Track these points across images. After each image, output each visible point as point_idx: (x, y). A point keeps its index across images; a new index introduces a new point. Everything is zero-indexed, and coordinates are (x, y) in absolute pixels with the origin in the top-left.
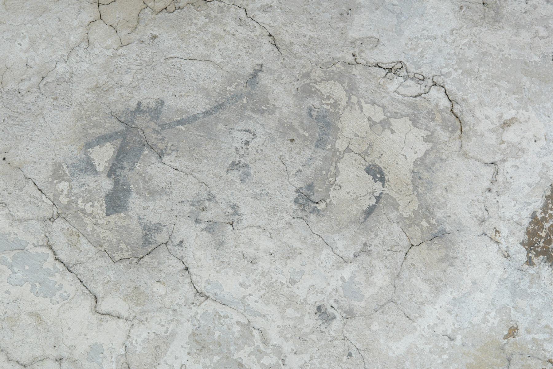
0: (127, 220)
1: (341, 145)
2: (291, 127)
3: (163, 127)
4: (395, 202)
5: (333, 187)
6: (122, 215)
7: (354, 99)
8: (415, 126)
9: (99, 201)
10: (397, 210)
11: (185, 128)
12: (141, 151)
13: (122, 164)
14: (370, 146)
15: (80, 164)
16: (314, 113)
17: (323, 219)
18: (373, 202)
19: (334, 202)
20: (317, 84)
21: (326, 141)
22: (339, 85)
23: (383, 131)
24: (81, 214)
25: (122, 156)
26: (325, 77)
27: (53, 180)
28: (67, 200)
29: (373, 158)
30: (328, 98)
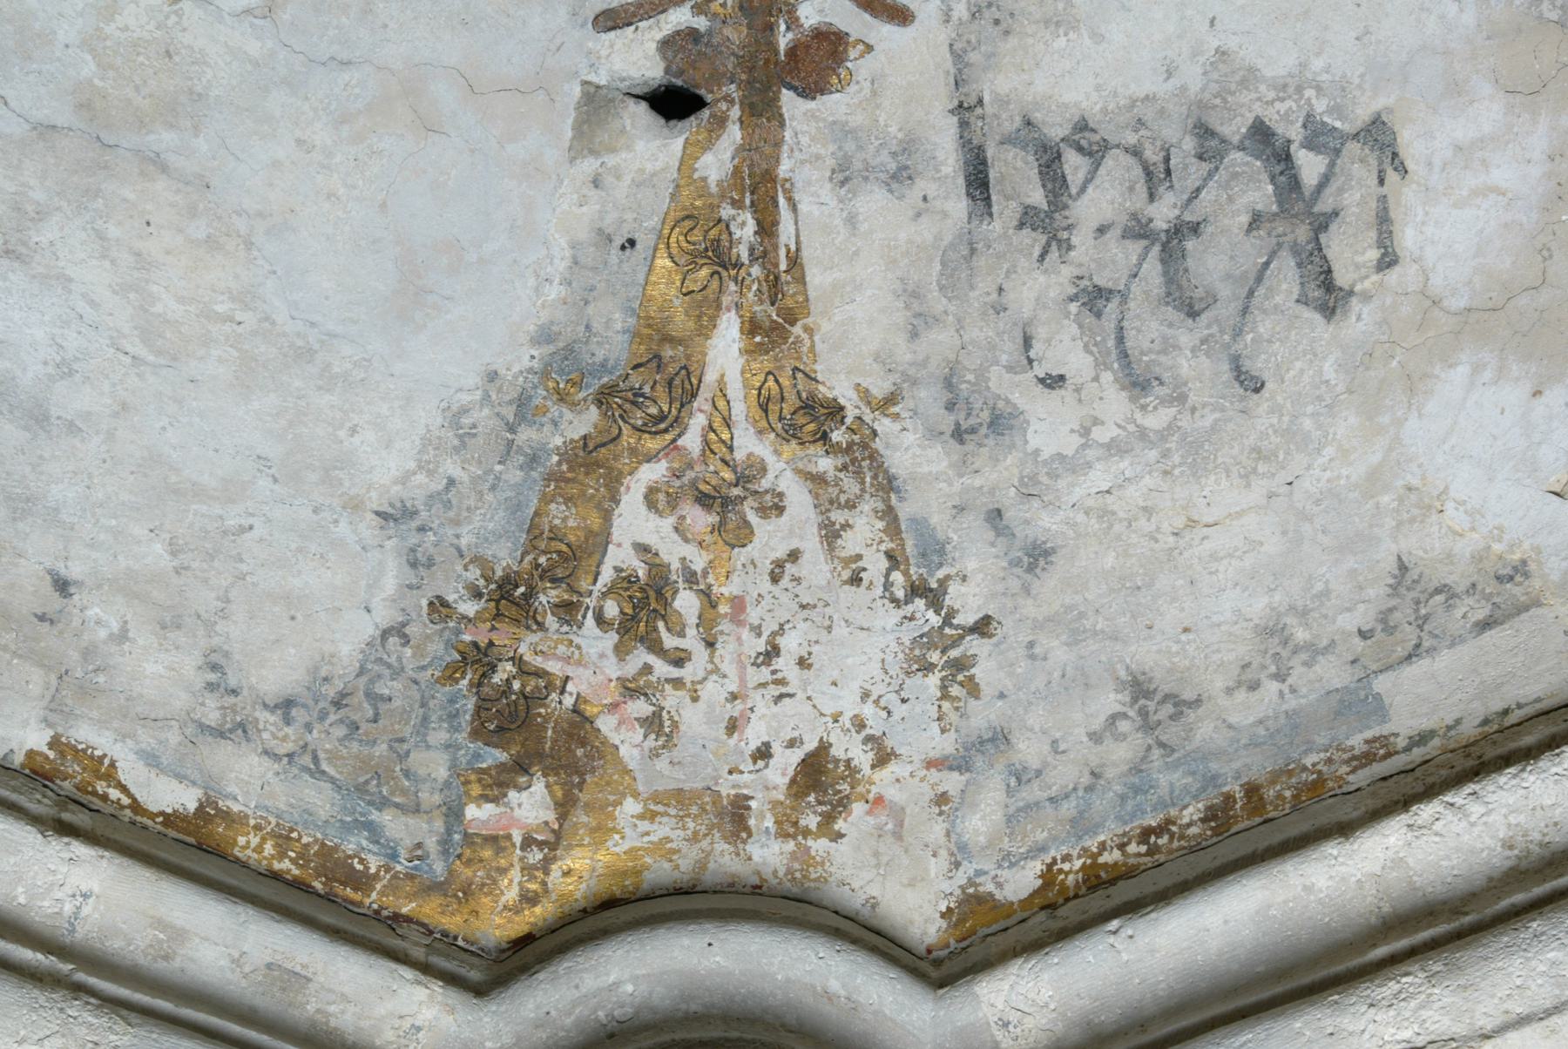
1: (1107, 377)
2: (1164, 352)
3: (1279, 245)
6: (1244, 130)
7: (1131, 428)
8: (1058, 454)
10: (1004, 367)
12: (1280, 204)
14: (1080, 400)
16: (1155, 383)
17: (1062, 297)
18: (1032, 354)
19: (1066, 322)
24: (1281, 95)
28: (1306, 96)
29: (1066, 393)
30: (1155, 408)
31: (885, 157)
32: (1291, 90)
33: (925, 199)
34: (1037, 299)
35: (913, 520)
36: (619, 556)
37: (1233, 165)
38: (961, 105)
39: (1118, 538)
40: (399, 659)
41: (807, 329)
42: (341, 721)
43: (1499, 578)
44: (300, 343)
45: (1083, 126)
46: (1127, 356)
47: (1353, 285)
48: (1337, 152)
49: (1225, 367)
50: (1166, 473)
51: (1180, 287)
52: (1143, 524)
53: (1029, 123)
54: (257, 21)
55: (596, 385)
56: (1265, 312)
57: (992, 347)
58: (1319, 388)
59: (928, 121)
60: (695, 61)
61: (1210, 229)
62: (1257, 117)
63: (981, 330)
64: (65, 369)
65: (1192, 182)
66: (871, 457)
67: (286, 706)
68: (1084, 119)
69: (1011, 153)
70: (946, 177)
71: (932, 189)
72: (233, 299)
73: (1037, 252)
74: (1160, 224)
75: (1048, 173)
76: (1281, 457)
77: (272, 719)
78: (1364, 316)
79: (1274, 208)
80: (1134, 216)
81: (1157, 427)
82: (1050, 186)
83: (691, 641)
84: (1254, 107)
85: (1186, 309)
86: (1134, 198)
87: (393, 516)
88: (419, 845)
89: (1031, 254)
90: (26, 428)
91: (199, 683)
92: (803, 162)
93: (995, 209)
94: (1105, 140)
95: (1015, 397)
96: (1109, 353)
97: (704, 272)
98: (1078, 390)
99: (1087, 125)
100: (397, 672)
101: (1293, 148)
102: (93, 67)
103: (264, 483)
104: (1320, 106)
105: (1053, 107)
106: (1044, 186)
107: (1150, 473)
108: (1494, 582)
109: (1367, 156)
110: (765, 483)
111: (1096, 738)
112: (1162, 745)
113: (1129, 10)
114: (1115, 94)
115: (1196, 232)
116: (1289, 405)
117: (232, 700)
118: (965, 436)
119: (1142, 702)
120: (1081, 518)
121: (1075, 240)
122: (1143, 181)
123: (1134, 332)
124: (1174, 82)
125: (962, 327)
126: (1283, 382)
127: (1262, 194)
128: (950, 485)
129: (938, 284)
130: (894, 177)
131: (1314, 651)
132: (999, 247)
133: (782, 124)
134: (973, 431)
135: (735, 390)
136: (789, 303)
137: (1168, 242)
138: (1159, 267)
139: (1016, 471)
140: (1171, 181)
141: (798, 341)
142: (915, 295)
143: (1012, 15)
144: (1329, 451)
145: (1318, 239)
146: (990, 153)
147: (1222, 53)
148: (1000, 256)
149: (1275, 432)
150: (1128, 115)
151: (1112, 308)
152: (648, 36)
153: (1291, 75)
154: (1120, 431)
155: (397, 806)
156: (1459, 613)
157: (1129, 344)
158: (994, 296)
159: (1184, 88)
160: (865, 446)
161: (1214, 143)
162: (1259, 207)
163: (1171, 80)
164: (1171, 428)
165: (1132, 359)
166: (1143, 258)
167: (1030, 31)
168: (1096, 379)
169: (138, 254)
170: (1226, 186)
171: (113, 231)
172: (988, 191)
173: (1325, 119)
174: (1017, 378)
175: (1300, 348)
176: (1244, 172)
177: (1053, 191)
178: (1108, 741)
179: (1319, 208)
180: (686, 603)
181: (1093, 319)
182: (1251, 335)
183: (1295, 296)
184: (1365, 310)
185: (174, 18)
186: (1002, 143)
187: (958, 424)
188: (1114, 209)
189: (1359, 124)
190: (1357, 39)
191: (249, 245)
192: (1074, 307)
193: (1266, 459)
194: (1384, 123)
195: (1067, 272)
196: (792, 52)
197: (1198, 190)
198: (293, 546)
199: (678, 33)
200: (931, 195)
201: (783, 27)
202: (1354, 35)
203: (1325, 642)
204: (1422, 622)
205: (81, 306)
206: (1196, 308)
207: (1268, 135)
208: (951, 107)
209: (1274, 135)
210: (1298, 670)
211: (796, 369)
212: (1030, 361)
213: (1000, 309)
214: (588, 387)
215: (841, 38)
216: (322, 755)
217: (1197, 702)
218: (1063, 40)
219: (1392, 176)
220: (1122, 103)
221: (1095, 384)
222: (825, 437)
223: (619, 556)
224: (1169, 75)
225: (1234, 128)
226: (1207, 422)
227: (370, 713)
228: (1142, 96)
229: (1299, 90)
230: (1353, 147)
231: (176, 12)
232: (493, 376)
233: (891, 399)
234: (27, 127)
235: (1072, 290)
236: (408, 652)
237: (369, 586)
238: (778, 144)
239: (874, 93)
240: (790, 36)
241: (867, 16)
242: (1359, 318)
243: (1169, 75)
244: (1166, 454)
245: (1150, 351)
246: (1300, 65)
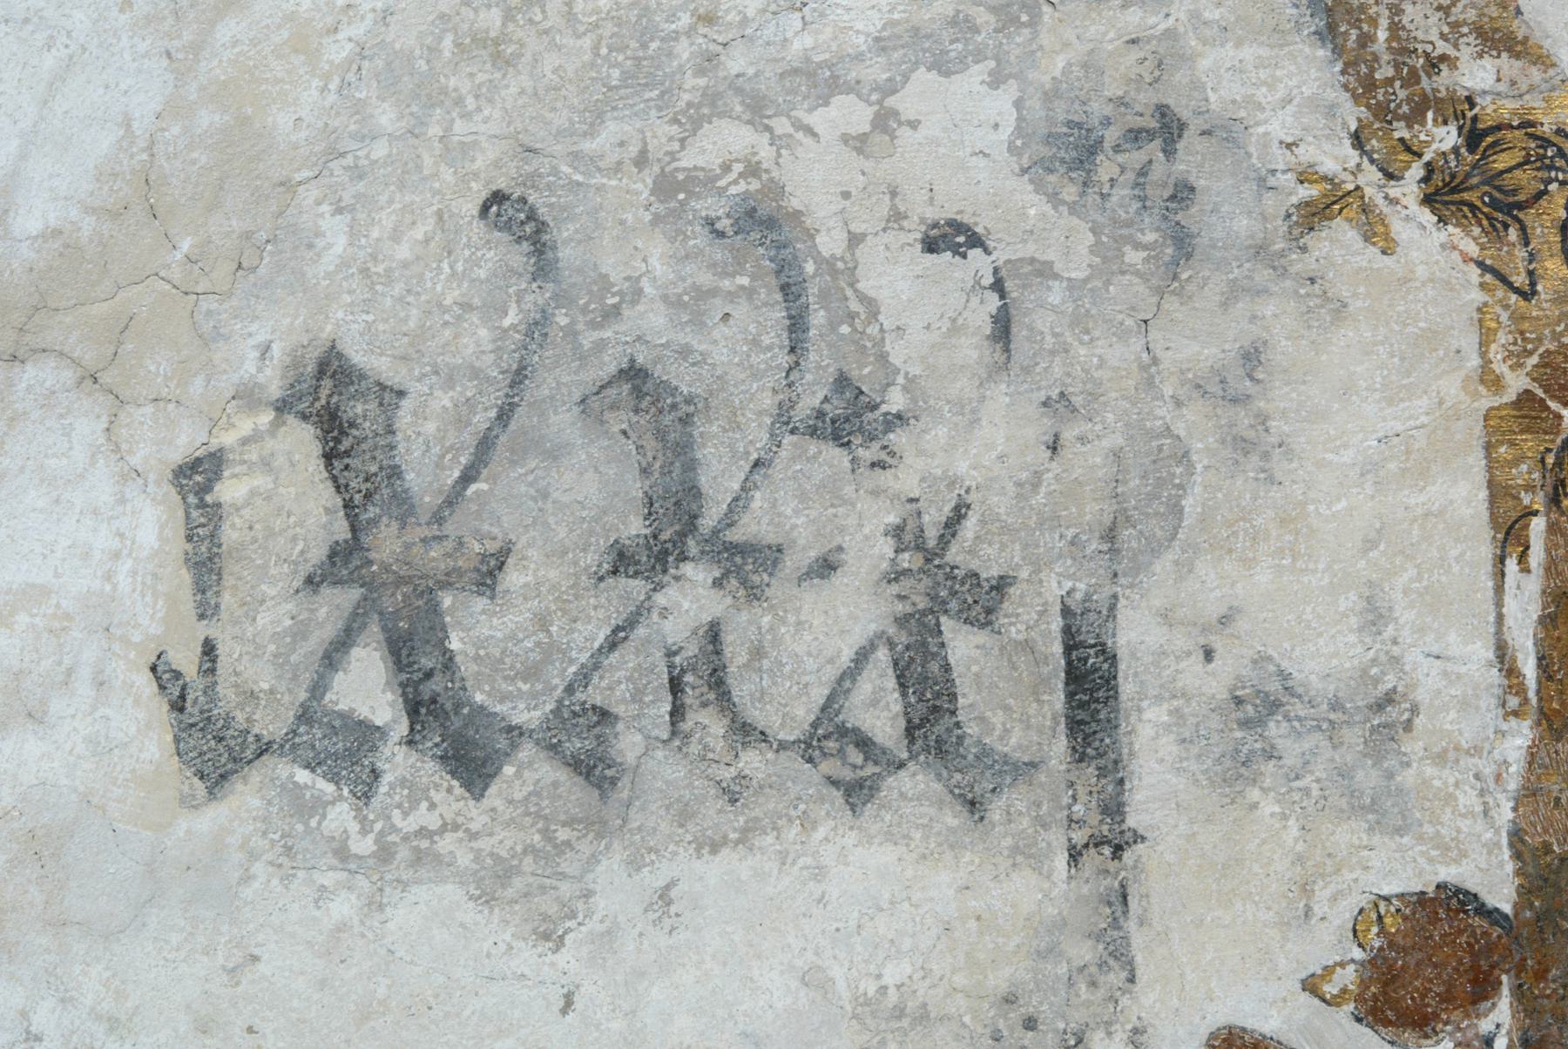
0: (526, 774)
1: (830, 243)
3: (438, 519)
4: (1037, 266)
5: (887, 342)
6: (508, 770)
7: (782, 126)
8: (947, 74)
9: (437, 787)
10: (1056, 276)
11: (486, 481)
12: (434, 609)
13: (420, 669)
14: (894, 194)
15: (335, 744)
16: (724, 224)
17: (921, 425)
18: (994, 302)
19: (915, 370)
20: (679, 160)
21: (795, 257)
22: (724, 123)
23: (892, 140)
24: (424, 844)
25: (404, 652)
26: (685, 130)
27: (306, 824)
28: (370, 839)
29: (923, 211)
30: (726, 168)
31: (1292, 751)
32: (403, 853)
33: (1208, 655)
34: (975, 422)
37: (534, 695)
38: (1118, 850)
41: (1496, 384)
45: (857, 793)
46: (784, 288)
47: (277, 424)
48: (305, 716)
49: (567, 254)
50: (709, 19)
51: (661, 435)
56: (476, 373)
57: (1080, 322)
59: (1191, 822)
61: (590, 559)
62: (478, 797)
63: (1102, 361)
65: (624, 662)
66: (1370, 85)
68: (853, 808)
69: (1014, 743)
70: (1159, 699)
71: (1192, 673)
73: (970, 527)
74: (698, 573)
75: (938, 695)
76: (448, 42)
79: (447, 600)
80: (754, 594)
81: (723, 124)
84: (485, 819)
85: (649, 386)
86: (752, 634)
89: (983, 522)
92: (1475, 751)
93: (1056, 624)
94: (810, 760)
95: (1036, 207)
96: (824, 296)
101: (403, 728)
104: (341, 817)
105: (917, 835)
106: (947, 668)
107: (745, 21)
109: (241, 706)
113: (745, 1035)
114: (783, 857)
115: (621, 555)
116: (428, 161)
118: (1154, 124)
121: (886, 547)
122: (732, 669)
123: (766, 340)
124: (654, 879)
125: (1144, 368)
126: (439, 215)
129: (1190, 467)
130: (1274, 706)
132: (1053, 541)
133: (1516, 837)
134: (1136, 136)
136: (1530, 444)
137: (682, 535)
138: (703, 480)
139: (1045, 39)
140: (671, 666)
141: (1516, 358)
142: (1244, 446)
144: (338, 51)
145: (354, 529)
146: (1060, 746)
147: (550, 936)
148: (1051, 520)
149: (459, 101)
150: (757, 812)
151: (812, 397)
153: (404, 885)
158: (1068, 435)
159: (635, 864)
160: (1383, 113)
161: (574, 745)
162: (480, 603)
163: (661, 883)
164: (692, 122)
165: (773, 282)
166: (739, 503)
167: (960, 1000)
168: (855, 240)
170: (551, 650)
172: (1069, 663)
173: (330, 788)
174: (1030, 250)
175: (398, 289)
176: (513, 680)
177: (928, 656)
179: (350, 596)
181: (854, 374)
182: (507, 322)
183: (406, 403)
184: (250, 367)
186: (1033, 765)
187: (1169, 152)
188: (798, 610)
189: (256, 775)
190: (255, 959)
192: (896, 401)
193: (480, 40)
195: (905, 480)
196: (1482, 990)
197: (612, 644)
202: (262, 968)
206: (626, 387)
207: (456, 758)
208: (1140, 847)
209: (443, 758)
211: (1528, 294)
212: (998, 286)
213: (1059, 404)
215: (1373, 1011)
218: (888, 980)
219: (186, 660)
220: (770, 839)
221: (857, 227)
222: (1474, 137)
224: (665, 895)
226: (612, 130)
228: (725, 851)
229: (385, 854)
230: (271, 725)
233: (1314, 215)
235: (897, 438)
238: (1529, 794)
239: (1306, 889)
240: (1486, 1026)
242: (265, 350)
243: (665, 895)
244: (708, 62)
245: (731, 296)
246: (381, 907)
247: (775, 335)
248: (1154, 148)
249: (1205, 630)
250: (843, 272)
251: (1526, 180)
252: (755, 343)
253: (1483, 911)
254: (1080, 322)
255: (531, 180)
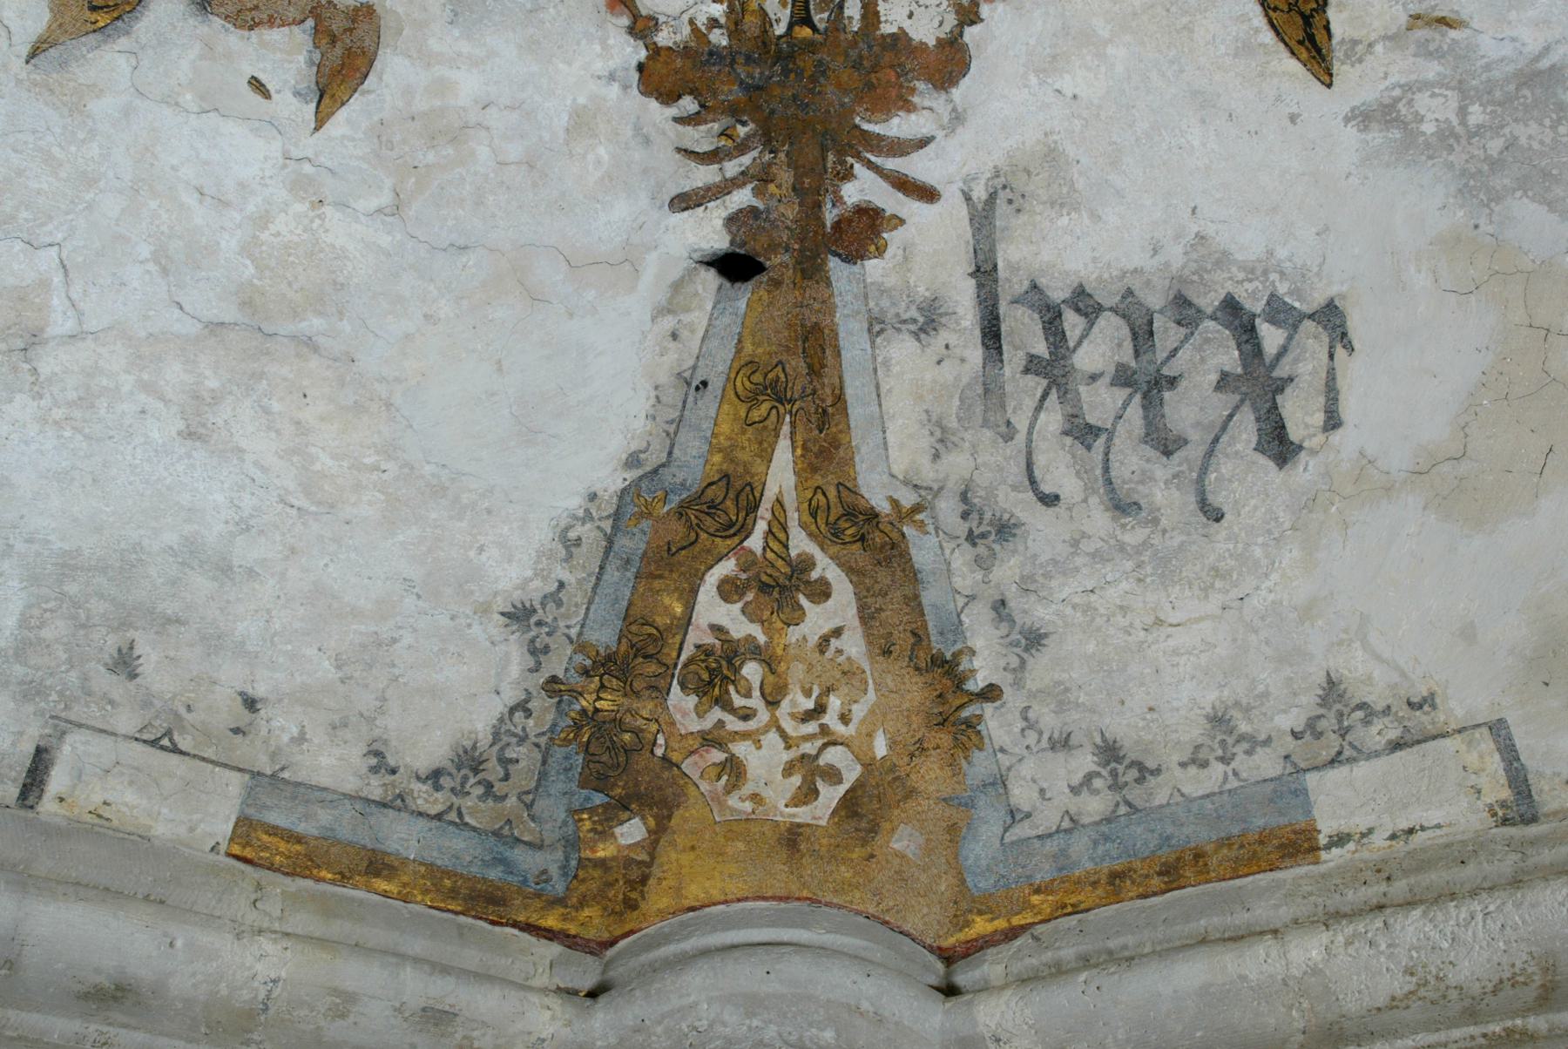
1: (1094, 500)
2: (1142, 482)
6: (1216, 303)
7: (1112, 542)
12: (1244, 366)
30: (1133, 527)
32: (1258, 273)
33: (947, 347)
35: (934, 606)
36: (698, 635)
37: (1207, 332)
39: (1099, 629)
40: (524, 729)
42: (479, 783)
43: (1409, 704)
44: (435, 482)
46: (1111, 483)
47: (1302, 441)
48: (1295, 327)
49: (1192, 499)
50: (1140, 580)
52: (1121, 621)
53: (1035, 286)
54: (387, 219)
55: (675, 500)
56: (1227, 456)
58: (1269, 523)
60: (755, 234)
62: (1229, 293)
64: (244, 526)
65: (1172, 343)
67: (435, 776)
68: (1081, 285)
70: (965, 329)
72: (378, 453)
76: (1235, 577)
77: (424, 788)
78: (1310, 468)
79: (1239, 370)
82: (1051, 339)
83: (756, 701)
85: (1162, 448)
87: (519, 615)
88: (545, 872)
90: (214, 579)
91: (364, 770)
93: (1005, 356)
96: (1096, 480)
97: (765, 407)
98: (1069, 509)
99: (1083, 291)
100: (522, 740)
101: (1258, 321)
102: (251, 270)
103: (410, 601)
104: (1282, 289)
106: (1047, 339)
107: (1127, 579)
108: (1405, 707)
110: (814, 575)
111: (1074, 790)
112: (1129, 804)
116: (1243, 534)
117: (389, 778)
119: (1113, 765)
120: (1069, 611)
124: (1160, 259)
127: (1230, 358)
128: (964, 579)
131: (1253, 743)
134: (983, 536)
135: (790, 501)
138: (1141, 411)
139: (1018, 571)
143: (1023, 196)
144: (1274, 577)
145: (1274, 399)
147: (1201, 238)
149: (1231, 555)
151: (1100, 443)
152: (715, 214)
153: (1259, 261)
154: (1102, 543)
155: (525, 843)
156: (1374, 730)
157: (1113, 474)
159: (1167, 264)
162: (1227, 368)
164: (1145, 544)
168: (1085, 500)
169: (298, 423)
170: (1200, 349)
171: (276, 406)
173: (1286, 299)
174: (1021, 496)
177: (1054, 344)
178: (1085, 792)
179: (1276, 373)
180: (752, 671)
183: (1253, 445)
184: (1311, 464)
185: (318, 222)
187: (971, 531)
191: (389, 405)
193: (1223, 577)
194: (1336, 307)
196: (837, 225)
197: (1176, 350)
198: (436, 649)
199: (741, 211)
200: (952, 343)
201: (829, 206)
202: (1314, 230)
203: (1263, 737)
204: (1343, 733)
205: (257, 474)
208: (970, 271)
209: (1242, 309)
210: (1240, 757)
214: (671, 502)
215: (878, 213)
216: (464, 811)
217: (1157, 772)
219: (1340, 352)
220: (1114, 274)
221: (1084, 505)
223: (698, 635)
224: (1155, 252)
225: (1209, 301)
227: (502, 773)
229: (1265, 272)
230: (1308, 325)
231: (319, 216)
232: (593, 497)
234: (200, 326)
236: (531, 722)
237: (498, 674)
239: (906, 258)
240: (835, 211)
241: (900, 195)
242: (1305, 469)
243: (1155, 252)
245: (1131, 481)
247: (1114, 465)
248: (976, 532)
249: (949, 356)
250: (1089, 490)
251: (843, 524)
252: (1122, 463)
253: (839, 256)
254: (1001, 469)
255: (1205, 526)
